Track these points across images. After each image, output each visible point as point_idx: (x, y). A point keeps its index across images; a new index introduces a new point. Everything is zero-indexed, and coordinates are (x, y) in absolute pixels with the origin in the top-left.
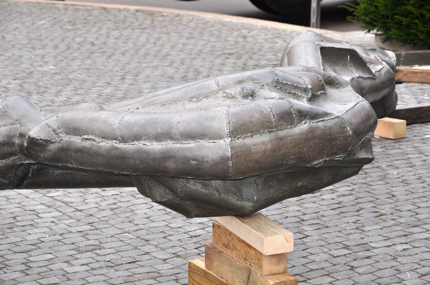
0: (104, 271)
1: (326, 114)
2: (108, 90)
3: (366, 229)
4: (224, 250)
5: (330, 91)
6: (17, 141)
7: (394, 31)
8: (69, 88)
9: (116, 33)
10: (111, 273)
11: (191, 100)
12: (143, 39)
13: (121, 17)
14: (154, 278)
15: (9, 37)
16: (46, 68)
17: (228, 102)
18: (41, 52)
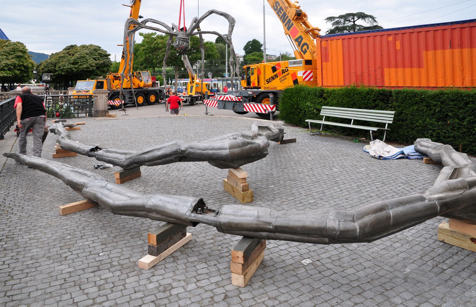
0: (204, 182)
6: (179, 151)
7: (287, 121)
9: (221, 123)
10: (206, 182)
12: (227, 124)
13: (223, 119)
15: (195, 124)
18: (202, 128)
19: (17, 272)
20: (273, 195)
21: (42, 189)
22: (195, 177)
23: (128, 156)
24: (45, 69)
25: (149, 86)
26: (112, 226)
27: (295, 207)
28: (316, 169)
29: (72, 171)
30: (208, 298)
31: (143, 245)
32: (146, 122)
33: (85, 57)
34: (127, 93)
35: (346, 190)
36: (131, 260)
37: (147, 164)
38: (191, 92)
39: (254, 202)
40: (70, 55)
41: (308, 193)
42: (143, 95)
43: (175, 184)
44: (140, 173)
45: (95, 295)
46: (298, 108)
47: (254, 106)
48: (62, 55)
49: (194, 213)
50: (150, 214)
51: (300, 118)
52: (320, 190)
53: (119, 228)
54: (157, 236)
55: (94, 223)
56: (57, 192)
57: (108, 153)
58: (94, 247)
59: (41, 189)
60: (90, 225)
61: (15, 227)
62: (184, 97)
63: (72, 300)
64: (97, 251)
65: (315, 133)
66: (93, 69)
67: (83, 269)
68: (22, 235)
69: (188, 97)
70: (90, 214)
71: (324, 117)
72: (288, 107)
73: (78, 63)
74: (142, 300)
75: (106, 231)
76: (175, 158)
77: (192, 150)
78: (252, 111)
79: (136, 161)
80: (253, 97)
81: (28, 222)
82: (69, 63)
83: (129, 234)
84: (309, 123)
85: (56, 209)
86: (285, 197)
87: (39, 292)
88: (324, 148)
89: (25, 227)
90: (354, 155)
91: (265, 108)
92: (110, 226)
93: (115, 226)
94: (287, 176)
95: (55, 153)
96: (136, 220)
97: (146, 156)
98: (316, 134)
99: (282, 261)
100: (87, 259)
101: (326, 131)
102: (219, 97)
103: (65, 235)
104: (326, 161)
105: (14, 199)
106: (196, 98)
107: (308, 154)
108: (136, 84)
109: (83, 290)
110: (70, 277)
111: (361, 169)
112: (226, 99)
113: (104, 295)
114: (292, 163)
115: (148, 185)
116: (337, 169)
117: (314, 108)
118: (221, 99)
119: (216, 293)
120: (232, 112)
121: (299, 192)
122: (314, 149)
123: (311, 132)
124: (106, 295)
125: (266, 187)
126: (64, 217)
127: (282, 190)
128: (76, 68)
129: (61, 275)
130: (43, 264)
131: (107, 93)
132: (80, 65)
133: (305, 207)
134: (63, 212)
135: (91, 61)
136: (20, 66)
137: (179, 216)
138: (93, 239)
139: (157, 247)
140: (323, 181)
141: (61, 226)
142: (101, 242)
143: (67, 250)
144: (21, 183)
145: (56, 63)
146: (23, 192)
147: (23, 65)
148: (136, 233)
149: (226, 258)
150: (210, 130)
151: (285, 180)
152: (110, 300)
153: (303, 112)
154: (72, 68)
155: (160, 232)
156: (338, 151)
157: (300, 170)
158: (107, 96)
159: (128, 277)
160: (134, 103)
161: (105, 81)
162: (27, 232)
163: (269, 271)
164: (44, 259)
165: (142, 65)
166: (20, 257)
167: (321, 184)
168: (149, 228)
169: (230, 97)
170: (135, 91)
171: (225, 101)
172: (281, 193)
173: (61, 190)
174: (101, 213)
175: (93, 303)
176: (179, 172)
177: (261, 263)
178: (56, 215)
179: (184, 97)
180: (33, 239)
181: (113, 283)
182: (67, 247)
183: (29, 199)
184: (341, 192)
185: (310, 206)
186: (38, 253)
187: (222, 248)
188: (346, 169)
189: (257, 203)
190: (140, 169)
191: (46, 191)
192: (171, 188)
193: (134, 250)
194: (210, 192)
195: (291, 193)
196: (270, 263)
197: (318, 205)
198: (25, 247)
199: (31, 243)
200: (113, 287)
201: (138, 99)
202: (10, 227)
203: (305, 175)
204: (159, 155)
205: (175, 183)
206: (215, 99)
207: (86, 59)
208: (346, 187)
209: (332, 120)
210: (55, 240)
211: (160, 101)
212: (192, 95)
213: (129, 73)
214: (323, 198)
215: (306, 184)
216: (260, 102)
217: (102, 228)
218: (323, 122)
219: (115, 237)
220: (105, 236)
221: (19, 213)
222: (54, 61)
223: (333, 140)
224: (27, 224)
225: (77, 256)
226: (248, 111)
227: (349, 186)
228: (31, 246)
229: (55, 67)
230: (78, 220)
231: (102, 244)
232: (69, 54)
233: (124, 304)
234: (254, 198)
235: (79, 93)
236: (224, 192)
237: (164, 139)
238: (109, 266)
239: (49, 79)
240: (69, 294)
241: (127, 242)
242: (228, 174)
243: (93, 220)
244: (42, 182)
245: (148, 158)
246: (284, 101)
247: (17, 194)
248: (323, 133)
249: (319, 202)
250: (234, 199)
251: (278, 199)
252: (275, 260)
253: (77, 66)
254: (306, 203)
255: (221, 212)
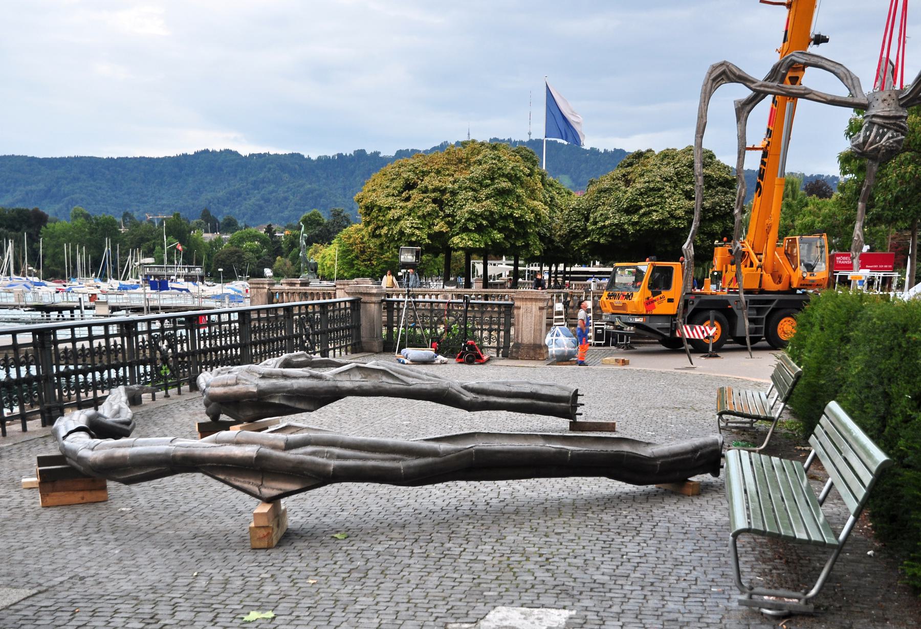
73: (641, 207)
128: (634, 224)
132: (644, 214)
136: (505, 218)
145: (589, 210)
147: (511, 215)
154: (624, 224)
207: (662, 197)
222: (585, 205)
229: (587, 219)
253: (635, 218)
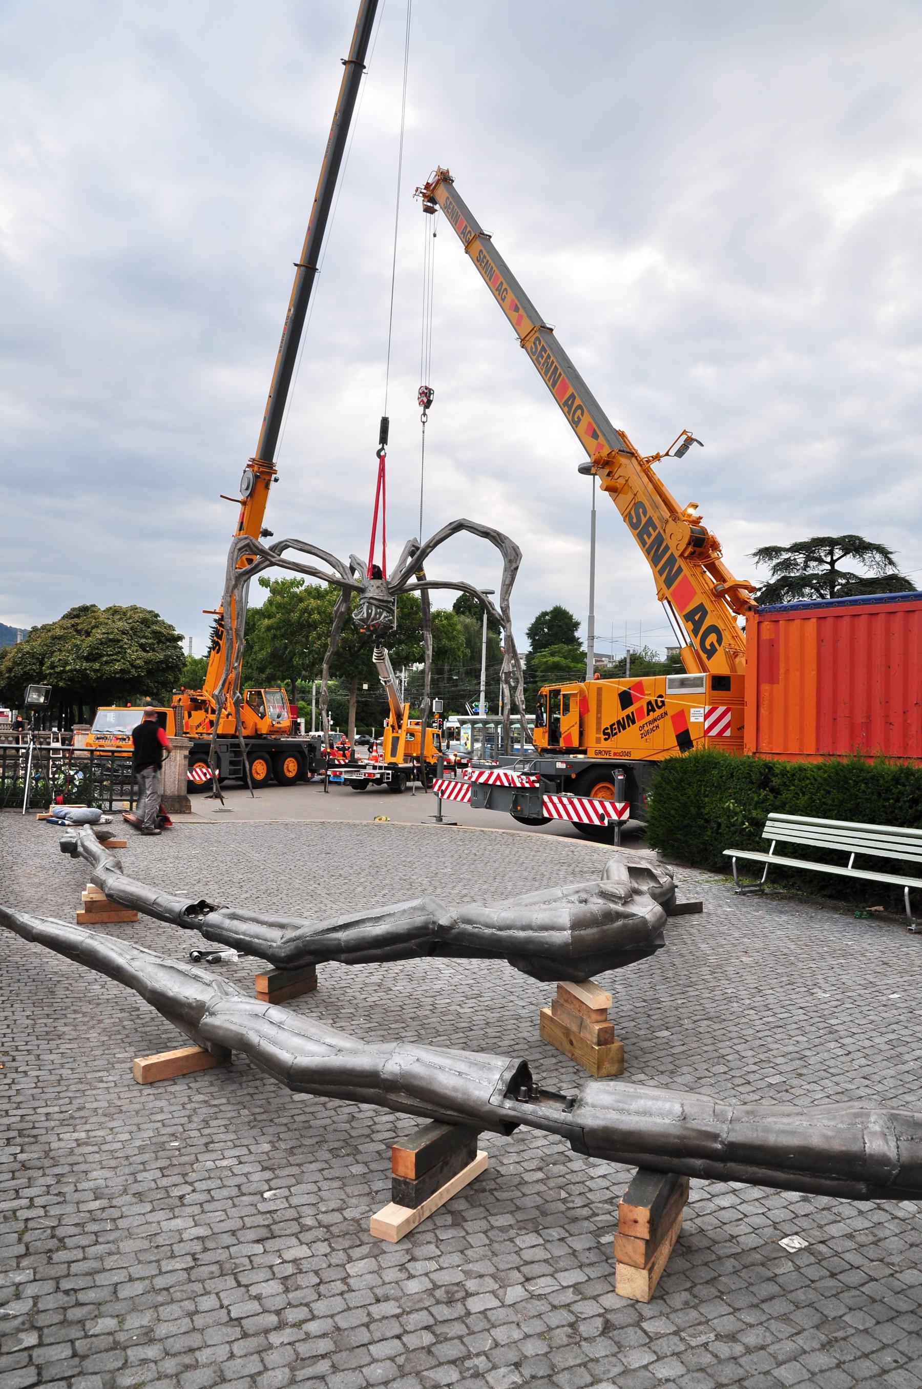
1: (634, 915)
2: (485, 887)
3: (657, 988)
4: (566, 1004)
5: (637, 898)
8: (462, 884)
9: (490, 848)
10: (488, 1014)
11: (544, 903)
12: (507, 852)
13: (493, 837)
14: (517, 1019)
15: (423, 849)
16: (446, 871)
17: (569, 905)
18: (443, 859)
19: (72, 1230)
20: (670, 1059)
21: (72, 1008)
22: (459, 998)
23: (290, 934)
24: (16, 668)
25: (281, 732)
26: (276, 1121)
27: (733, 1092)
28: (771, 991)
29: (162, 965)
30: (563, 1326)
31: (368, 1176)
32: (293, 836)
33: (119, 641)
34: (224, 748)
35: (860, 1054)
36: (348, 1213)
37: (343, 956)
38: (394, 753)
39: (626, 1074)
40: (79, 632)
41: (762, 1057)
42: (267, 756)
43: (413, 1015)
44: (315, 979)
45: (279, 1303)
46: (700, 815)
47: (572, 803)
48: (59, 632)
49: (510, 1098)
50: (392, 1097)
51: (704, 844)
52: (791, 1048)
53: (295, 1126)
54: (417, 1155)
55: (229, 1111)
56: (113, 1020)
57: (235, 922)
58: (246, 1175)
59: (69, 1007)
60: (219, 1116)
61: (35, 1109)
62: (375, 768)
63: (224, 1311)
64: (255, 1185)
65: (747, 889)
66: (139, 676)
67: (233, 1233)
68: (57, 1131)
69: (386, 768)
70: (212, 1085)
71: (774, 843)
72: (673, 812)
74: (400, 1323)
75: (264, 1134)
76: (420, 946)
77: (469, 927)
78: (565, 817)
79: (312, 947)
80: (568, 778)
81: (62, 1095)
82: (78, 657)
83: (326, 1146)
84: (734, 859)
85: (123, 1065)
86: (705, 1066)
87: (139, 1287)
88: (779, 932)
89: (57, 1109)
90: (863, 955)
91: (601, 811)
92: (271, 1121)
93: (284, 1121)
94: (698, 1008)
95: (83, 912)
96: (335, 1109)
97: (342, 935)
98: (751, 892)
99: (728, 1237)
100: (234, 1206)
101: (773, 882)
102: (477, 773)
103: (165, 1139)
104: (793, 968)
105: (9, 1031)
106: (407, 774)
107: (740, 948)
108: (250, 725)
109: (247, 1286)
110: (205, 1250)
111: (891, 996)
112: (495, 781)
113: (301, 1304)
114: (705, 970)
115: (341, 1015)
116: (825, 992)
117: (744, 816)
118: (481, 780)
119: (581, 1313)
120: (506, 817)
121: (737, 1052)
122: (754, 935)
123: (738, 884)
124: (307, 1305)
125: (650, 1036)
126: (147, 1091)
127: (694, 1045)
128: (96, 671)
129: (182, 1245)
130: (128, 1213)
131: (186, 747)
132: (107, 663)
133: (760, 1093)
134: (145, 1077)
135: (134, 654)
137: (471, 1104)
138: (237, 1152)
139: (417, 1184)
140: (795, 1026)
141: (147, 1113)
142: (259, 1162)
143: (178, 1179)
144: (15, 987)
145: (44, 655)
146: (28, 1013)
148: (341, 1144)
149: (586, 1223)
150: (466, 867)
151: (695, 1018)
152: (319, 1318)
153: (712, 828)
154: (86, 669)
155: (423, 1145)
156: (817, 942)
157: (729, 991)
158: (185, 757)
159: (350, 1260)
160: (244, 779)
161: (169, 711)
162: (66, 1123)
163: (700, 1262)
164: (128, 1198)
165: (262, 670)
166: (68, 1189)
167: (790, 1033)
168: (373, 1132)
169: (506, 775)
170: (247, 745)
171: (494, 785)
172: (689, 1053)
173: (120, 1015)
174: (240, 1084)
175: (279, 1322)
176: (414, 984)
177: (677, 1242)
178: (126, 1083)
179: (375, 768)
180: (87, 1144)
181: (316, 1273)
182: (176, 1170)
183: (47, 1033)
184: (848, 1058)
185: (772, 1093)
186: (110, 1183)
187: (570, 1195)
188: (848, 994)
189: (634, 1078)
190: (315, 969)
191: (84, 1014)
192: (403, 1025)
193: (349, 1190)
194: (507, 1043)
195: (717, 1054)
196: (698, 1242)
197: (792, 1091)
198: (71, 1165)
199: (83, 1155)
200: (318, 1284)
201: (254, 767)
202: (22, 1106)
203: (744, 1007)
204: (377, 936)
205: (409, 1011)
206: (466, 778)
207: (121, 647)
208: (860, 1043)
209: (793, 853)
210: (141, 1149)
211: (309, 775)
212: (395, 764)
213: (234, 693)
214: (804, 1071)
215: (751, 1031)
216: (587, 794)
217: (252, 1124)
218: (770, 858)
219: (291, 1151)
220: (266, 1147)
221: (32, 1070)
222: (38, 650)
223: (797, 908)
224: (61, 1102)
225: (209, 1198)
226: (555, 815)
227: (867, 1043)
228: (86, 1162)
229: (42, 664)
230: (186, 1099)
231: (264, 1169)
232: (76, 631)
233: (357, 1330)
234: (626, 1065)
235: (102, 742)
236: (539, 1043)
237: (351, 888)
238: (295, 1228)
239: (42, 700)
240: (213, 1296)
241: (325, 1165)
242: (554, 995)
243: (224, 1101)
244: (68, 989)
245: (347, 941)
246: (660, 795)
247: (15, 1018)
248: (767, 890)
249: (795, 1082)
250: (573, 1064)
251: (685, 1069)
252: (710, 1234)
253: (97, 666)
254: (762, 1084)
255: (581, 1100)
